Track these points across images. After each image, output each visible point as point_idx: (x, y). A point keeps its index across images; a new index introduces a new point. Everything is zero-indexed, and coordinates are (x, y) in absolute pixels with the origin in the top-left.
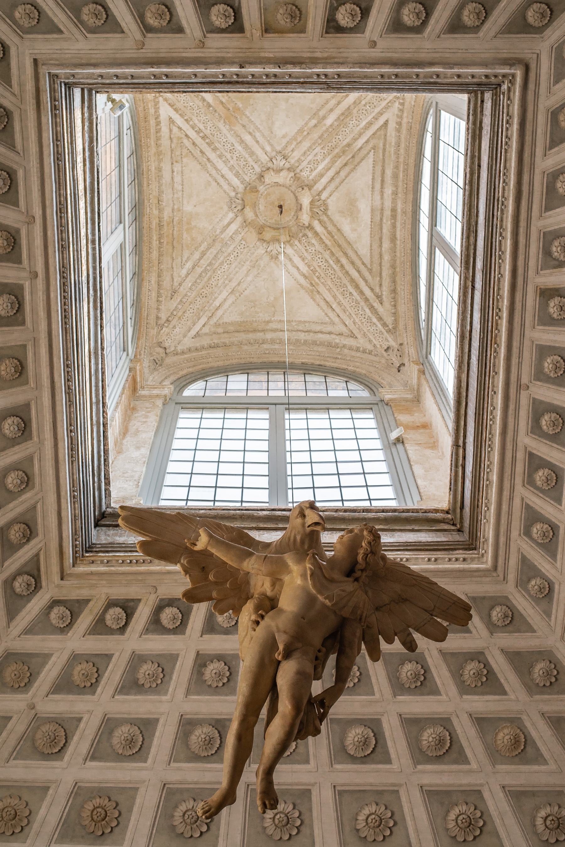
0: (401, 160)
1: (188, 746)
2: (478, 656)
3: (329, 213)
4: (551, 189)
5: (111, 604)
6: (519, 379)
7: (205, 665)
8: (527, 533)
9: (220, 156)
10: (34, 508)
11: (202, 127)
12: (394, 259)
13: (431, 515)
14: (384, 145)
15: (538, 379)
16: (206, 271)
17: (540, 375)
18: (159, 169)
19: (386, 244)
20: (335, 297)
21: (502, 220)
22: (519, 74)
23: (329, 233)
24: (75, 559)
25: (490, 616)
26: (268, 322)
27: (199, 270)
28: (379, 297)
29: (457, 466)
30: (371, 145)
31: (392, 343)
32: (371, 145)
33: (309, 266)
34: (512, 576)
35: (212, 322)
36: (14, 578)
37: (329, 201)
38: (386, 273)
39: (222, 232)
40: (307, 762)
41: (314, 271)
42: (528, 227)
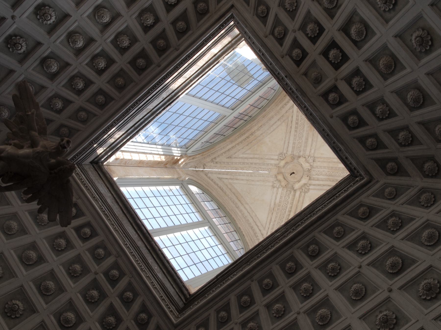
3: (306, 194)
4: (333, 227)
9: (295, 135)
11: (300, 119)
13: (184, 289)
16: (247, 163)
17: (260, 282)
18: (272, 117)
20: (275, 221)
23: (299, 201)
26: (247, 204)
27: (246, 161)
33: (280, 202)
35: (230, 181)
37: (311, 191)
39: (267, 159)
40: (47, 303)
41: (279, 206)
42: (312, 231)
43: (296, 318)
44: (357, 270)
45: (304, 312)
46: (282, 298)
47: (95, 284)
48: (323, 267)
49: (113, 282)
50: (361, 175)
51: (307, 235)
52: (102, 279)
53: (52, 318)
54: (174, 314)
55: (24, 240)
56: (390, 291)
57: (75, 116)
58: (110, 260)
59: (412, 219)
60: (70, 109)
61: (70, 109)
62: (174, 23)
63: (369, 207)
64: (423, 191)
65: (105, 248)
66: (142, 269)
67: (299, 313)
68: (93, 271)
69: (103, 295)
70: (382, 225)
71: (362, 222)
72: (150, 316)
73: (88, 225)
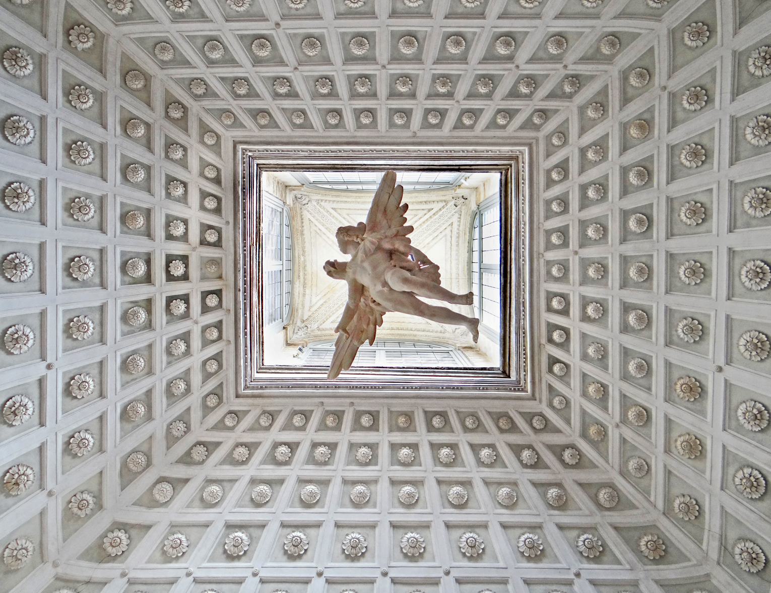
1: (642, 330)
2: (583, 152)
4: (301, 126)
5: (550, 371)
6: (409, 137)
7: (589, 317)
8: (504, 127)
10: (489, 413)
15: (409, 127)
17: (406, 126)
21: (320, 152)
22: (240, 147)
24: (523, 390)
25: (558, 146)
34: (532, 134)
36: (534, 428)
42: (323, 137)
43: (389, 63)
44: (300, 68)
45: (377, 64)
46: (393, 94)
47: (585, 241)
48: (333, 94)
49: (564, 232)
50: (243, 154)
51: (330, 137)
54: (523, 158)
56: (278, 24)
57: (479, 427)
58: (551, 255)
59: (223, 79)
60: (478, 438)
61: (477, 438)
62: (302, 428)
63: (256, 119)
64: (197, 97)
65: (549, 273)
67: (384, 67)
68: (577, 257)
70: (252, 94)
71: (271, 111)
72: (548, 172)
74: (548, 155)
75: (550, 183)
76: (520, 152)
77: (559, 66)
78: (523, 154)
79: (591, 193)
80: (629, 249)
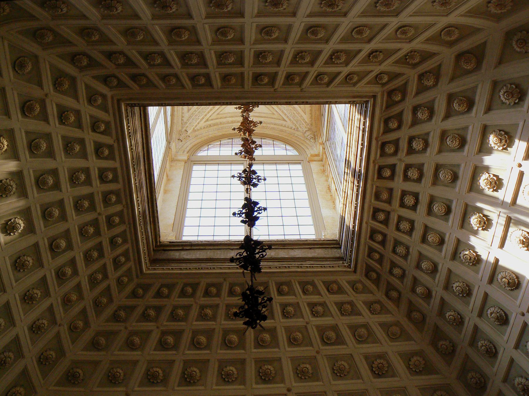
0: (268, 125)
12: (224, 123)
14: (274, 118)
19: (230, 119)
28: (207, 120)
29: (182, 245)
30: (275, 113)
31: (189, 132)
32: (275, 113)
38: (218, 121)
52: (102, 220)
53: (46, 241)
54: (146, 265)
55: (49, 164)
58: (118, 208)
66: (140, 224)
69: (98, 233)
73: (114, 170)
74: (129, 270)
75: (126, 254)
76: (149, 269)
77: (130, 328)
78: (147, 267)
79: (95, 254)
80: (61, 227)
